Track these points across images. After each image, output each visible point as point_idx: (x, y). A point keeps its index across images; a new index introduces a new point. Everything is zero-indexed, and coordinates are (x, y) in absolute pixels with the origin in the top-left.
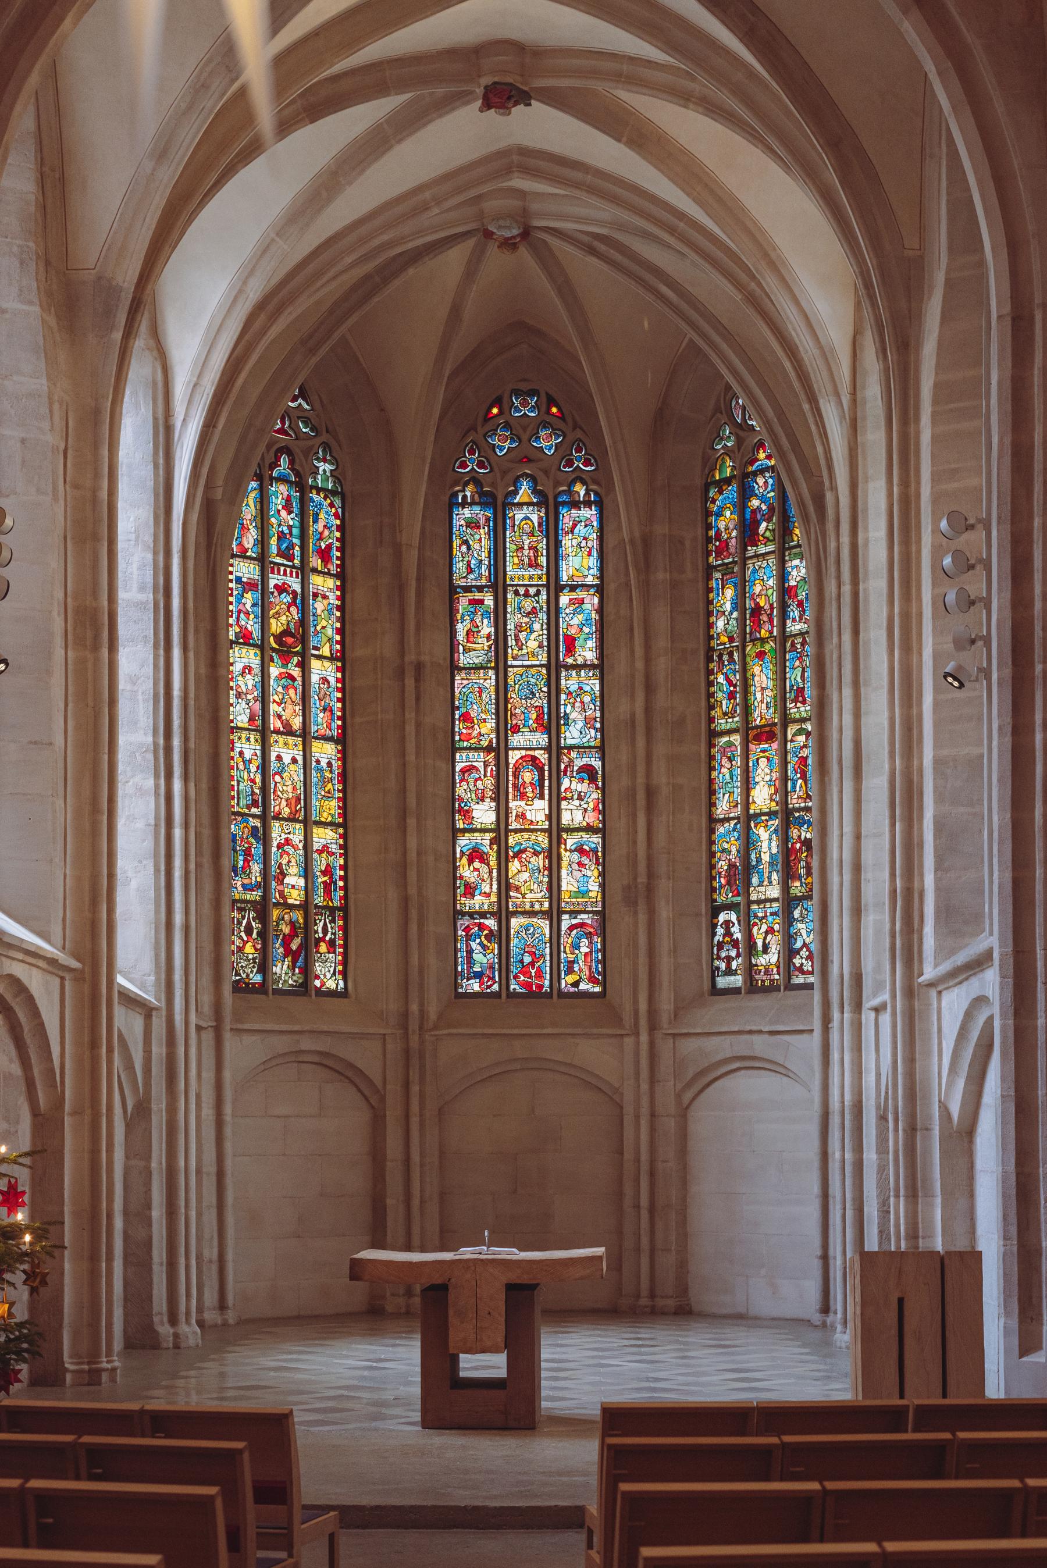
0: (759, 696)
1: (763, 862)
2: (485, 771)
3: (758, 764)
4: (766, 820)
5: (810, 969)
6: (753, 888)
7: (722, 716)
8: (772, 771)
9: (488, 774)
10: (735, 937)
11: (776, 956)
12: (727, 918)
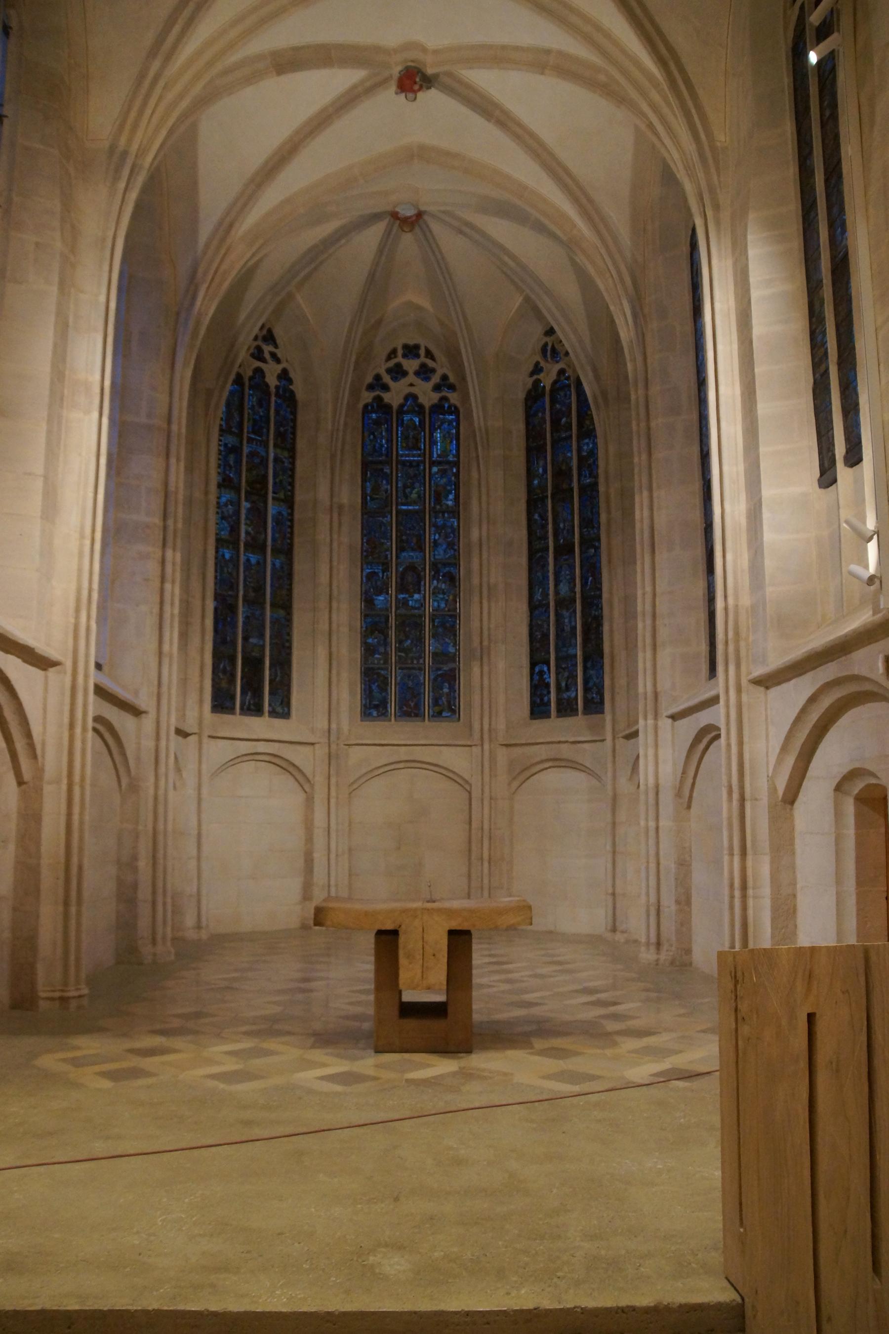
2: (383, 576)
9: (385, 577)
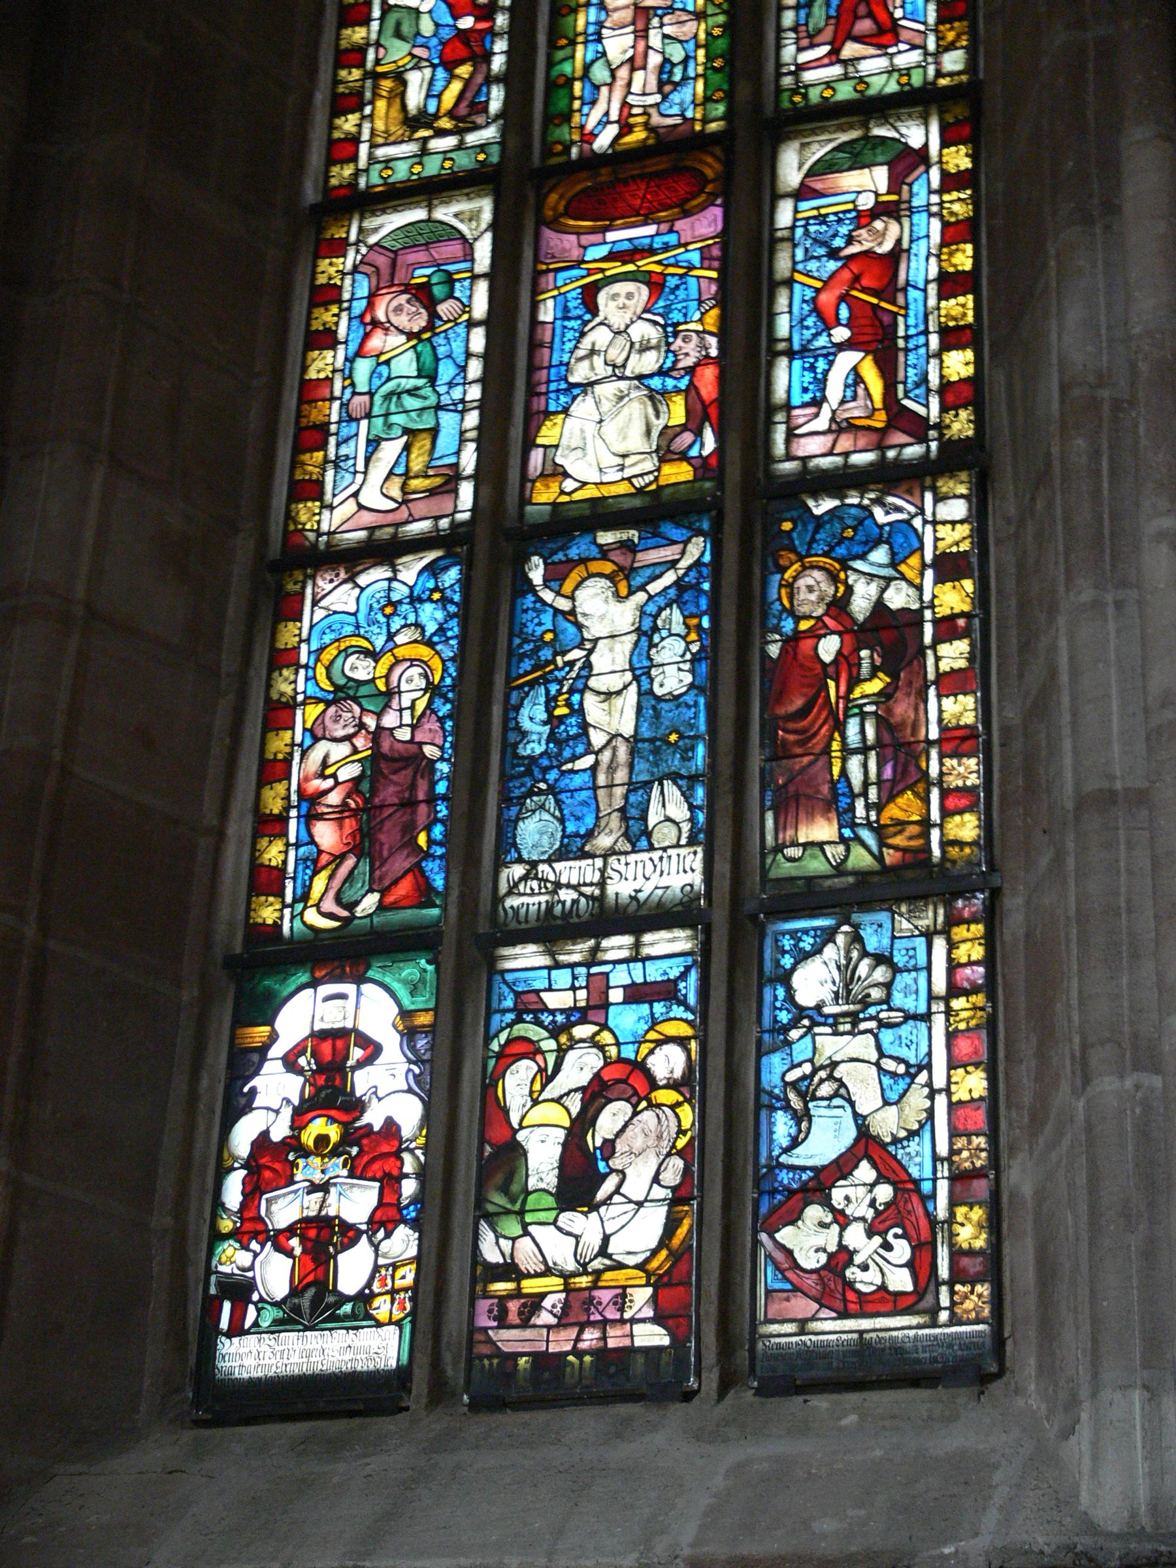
0: (618, 45)
1: (597, 739)
3: (593, 310)
4: (628, 547)
5: (901, 1281)
6: (518, 871)
7: (397, 130)
8: (671, 330)
10: (374, 1117)
11: (653, 1221)
12: (333, 1016)
